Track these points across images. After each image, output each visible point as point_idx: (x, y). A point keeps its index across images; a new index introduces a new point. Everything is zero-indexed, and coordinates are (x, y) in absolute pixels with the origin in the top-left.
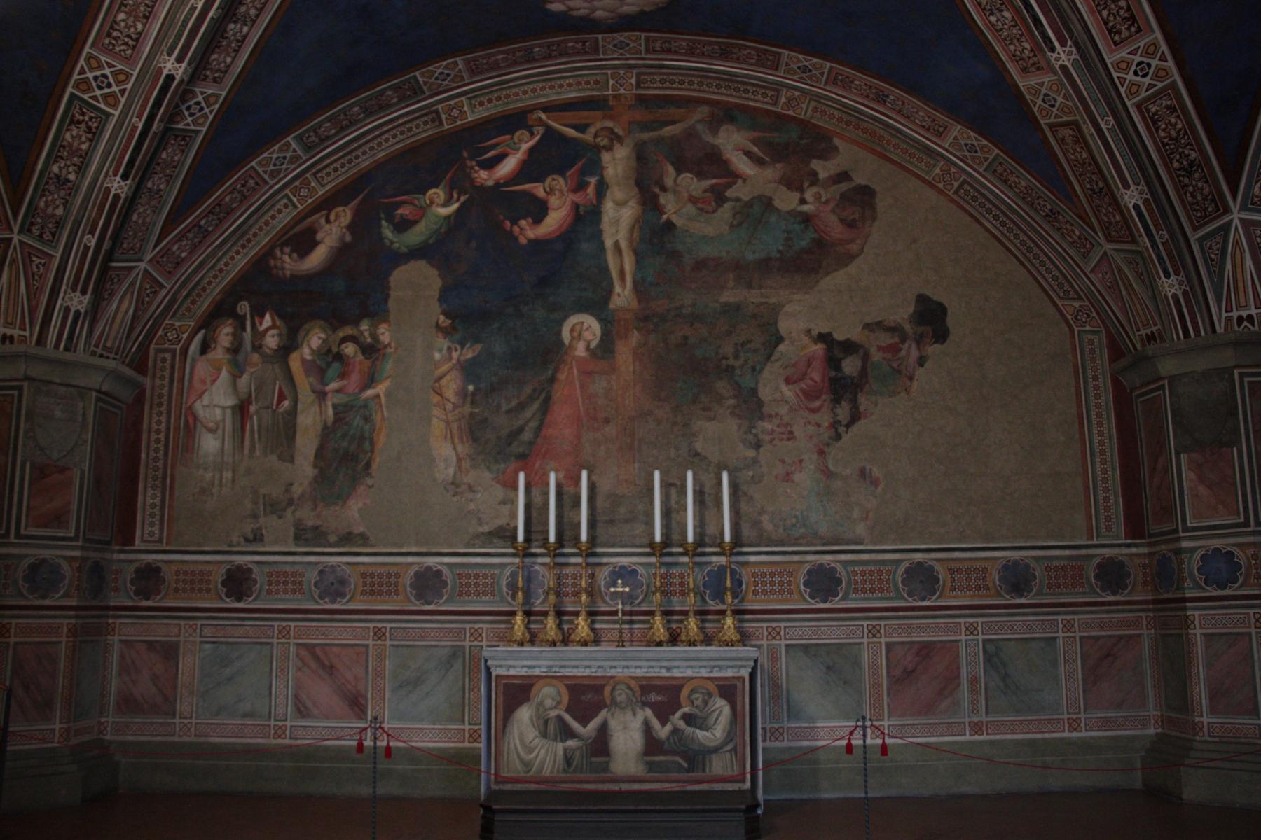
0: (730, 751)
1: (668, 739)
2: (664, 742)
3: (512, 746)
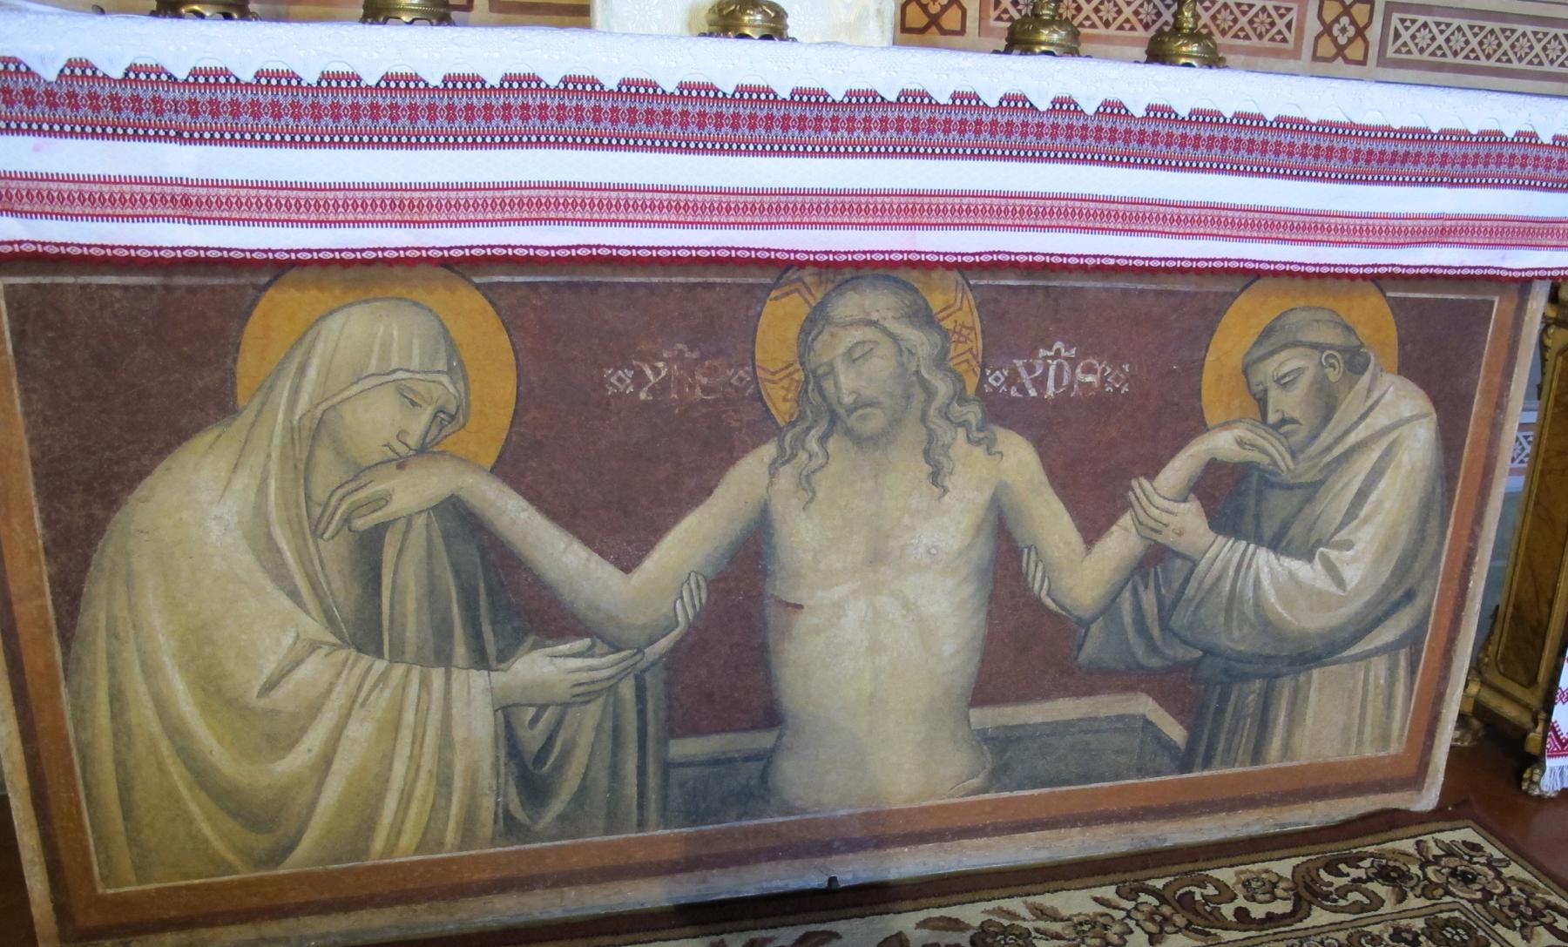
0: (1390, 649)
1: (1110, 606)
2: (1085, 624)
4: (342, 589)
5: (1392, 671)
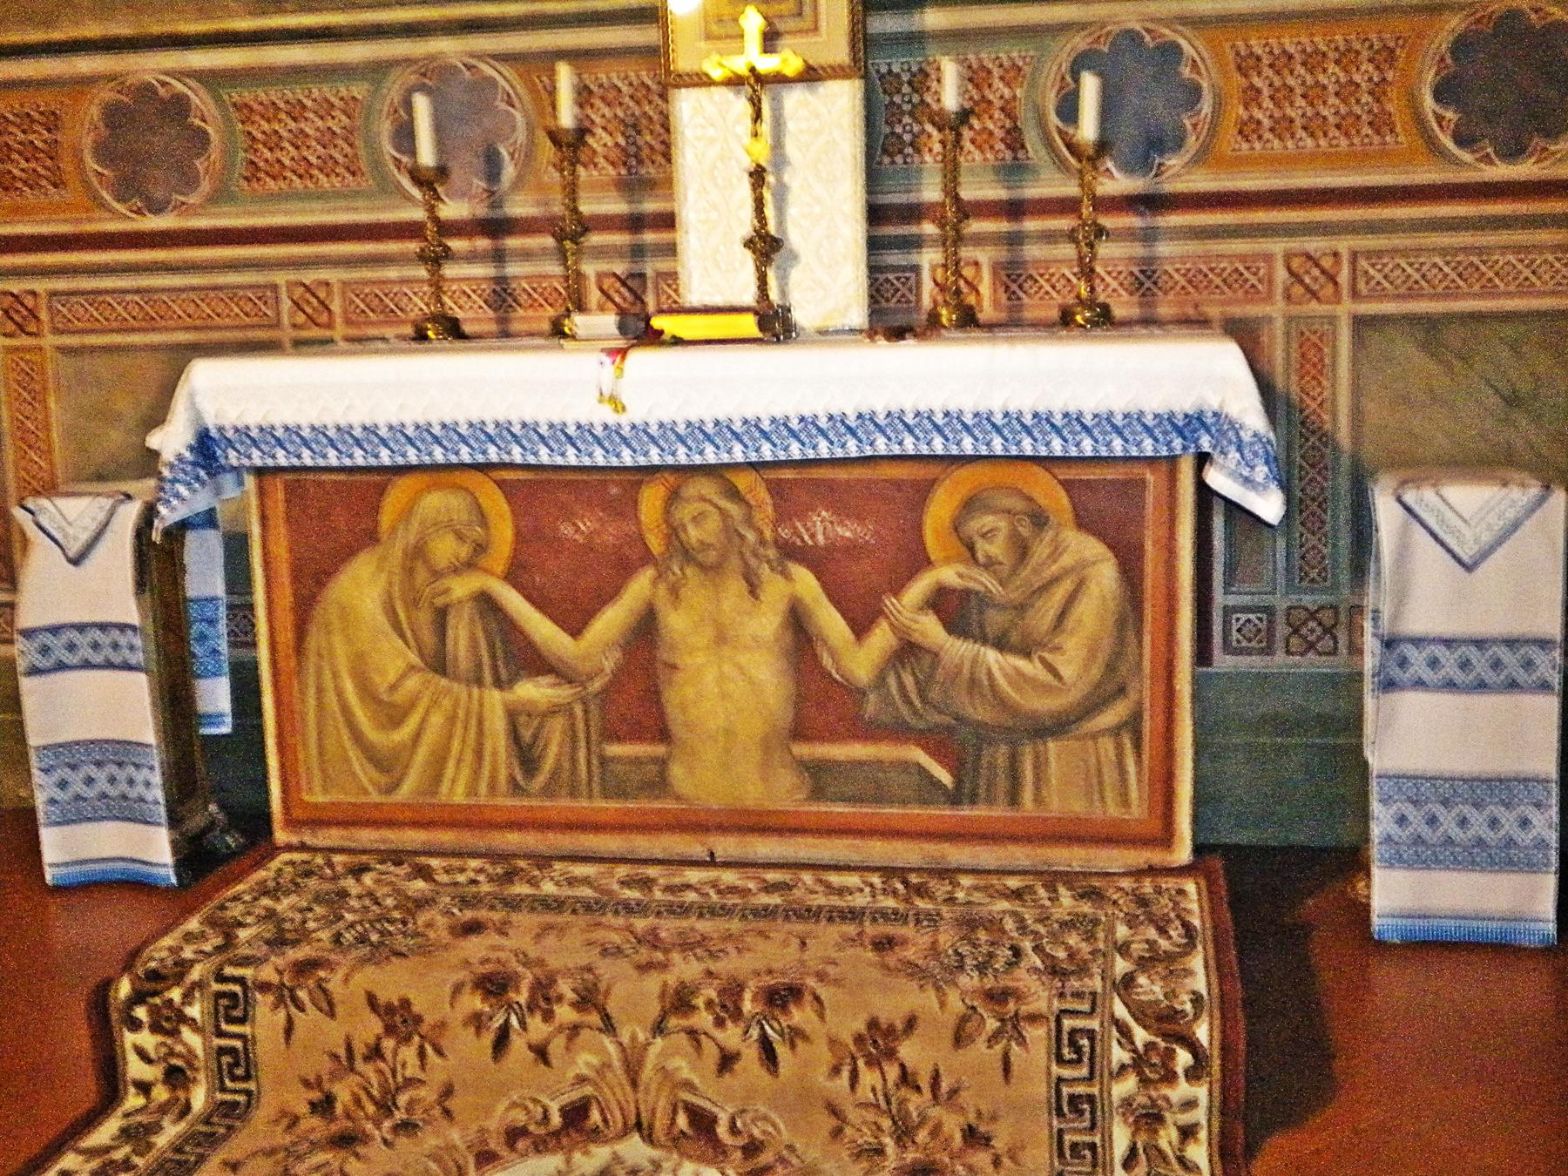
0: (1115, 731)
1: (880, 681)
2: (863, 693)
3: (331, 698)
4: (429, 638)
5: (1119, 748)
